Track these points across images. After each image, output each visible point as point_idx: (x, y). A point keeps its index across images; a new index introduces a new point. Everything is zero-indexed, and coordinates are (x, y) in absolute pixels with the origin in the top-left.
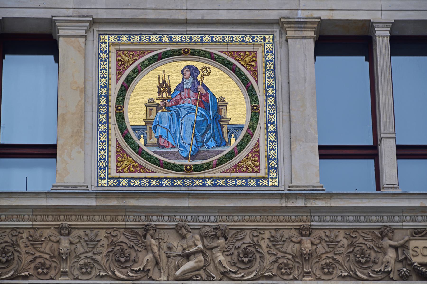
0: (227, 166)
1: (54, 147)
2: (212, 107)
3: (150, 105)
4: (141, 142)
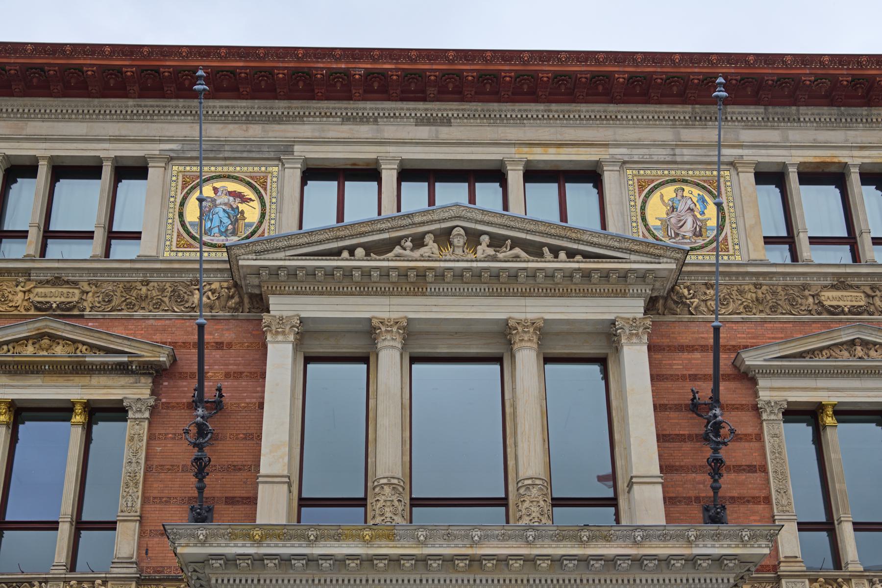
1: (140, 233)
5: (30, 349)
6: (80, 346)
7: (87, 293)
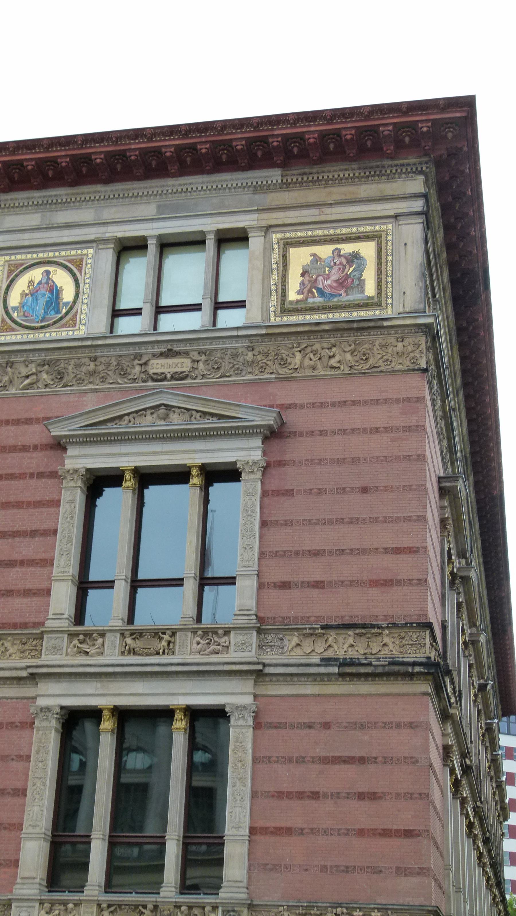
0: (58, 325)
2: (55, 292)
3: (24, 295)
4: (15, 315)
5: (149, 418)
6: (194, 413)
7: (198, 361)
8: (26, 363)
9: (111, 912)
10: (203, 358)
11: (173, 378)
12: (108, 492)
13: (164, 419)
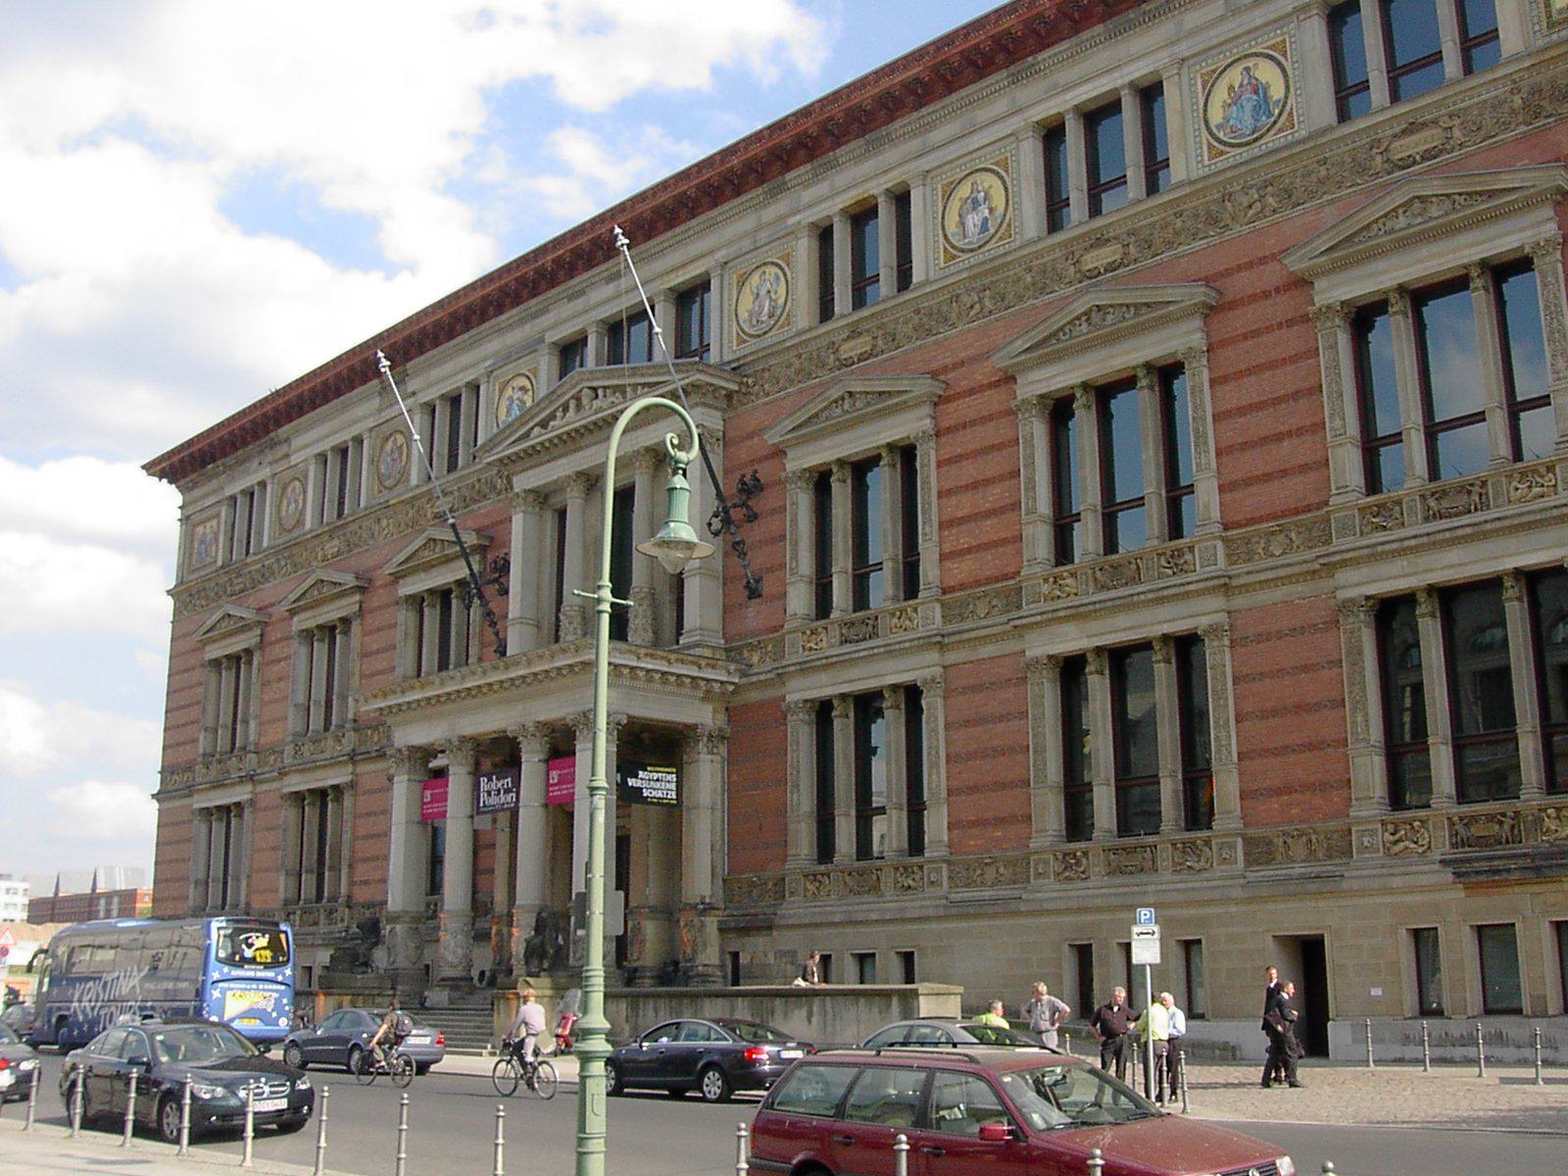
0: (1272, 132)
2: (1259, 89)
4: (1221, 135)
6: (1456, 197)
7: (1451, 128)
8: (1245, 190)
9: (1466, 825)
10: (1457, 122)
11: (1424, 159)
12: (1380, 321)
13: (1421, 215)
